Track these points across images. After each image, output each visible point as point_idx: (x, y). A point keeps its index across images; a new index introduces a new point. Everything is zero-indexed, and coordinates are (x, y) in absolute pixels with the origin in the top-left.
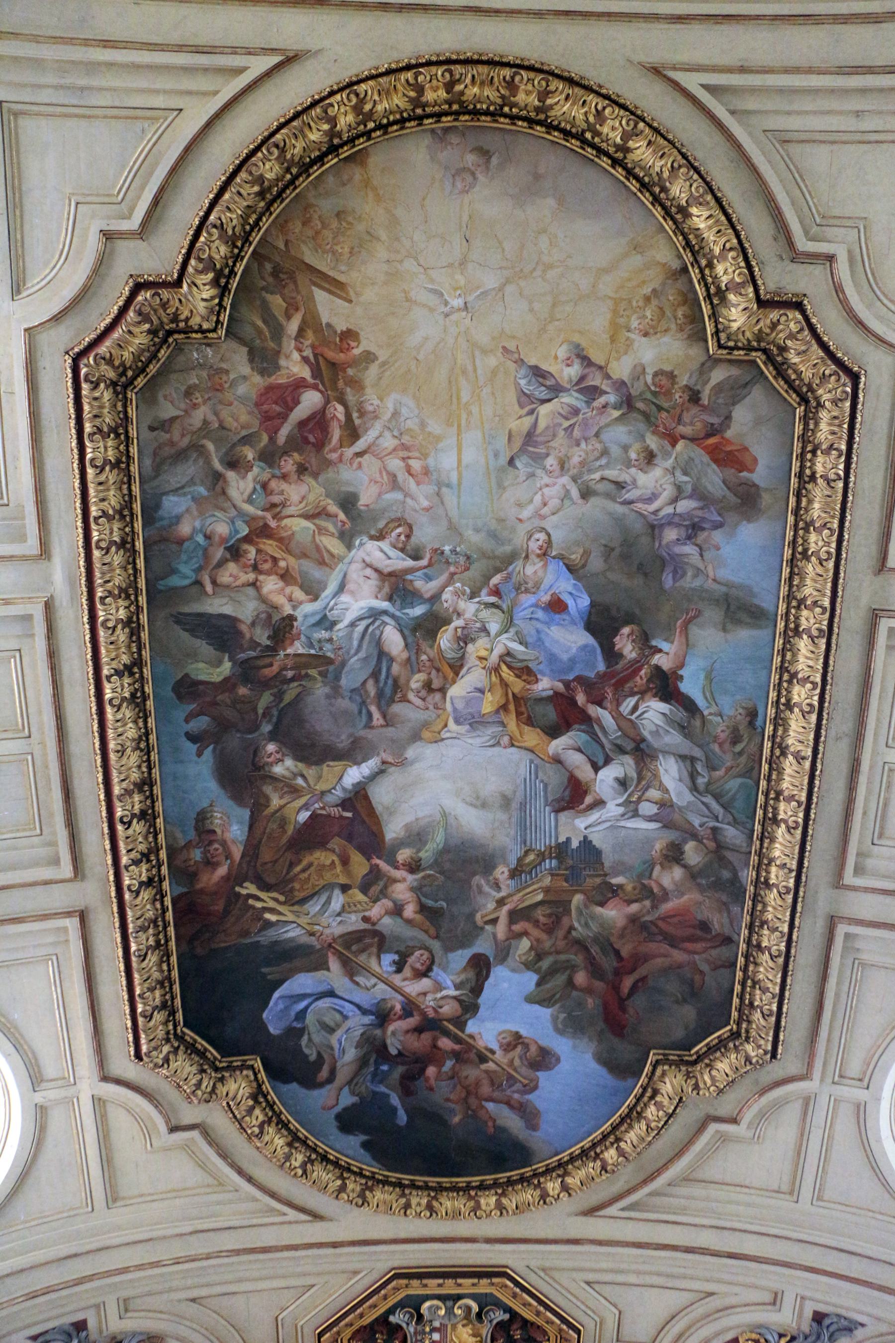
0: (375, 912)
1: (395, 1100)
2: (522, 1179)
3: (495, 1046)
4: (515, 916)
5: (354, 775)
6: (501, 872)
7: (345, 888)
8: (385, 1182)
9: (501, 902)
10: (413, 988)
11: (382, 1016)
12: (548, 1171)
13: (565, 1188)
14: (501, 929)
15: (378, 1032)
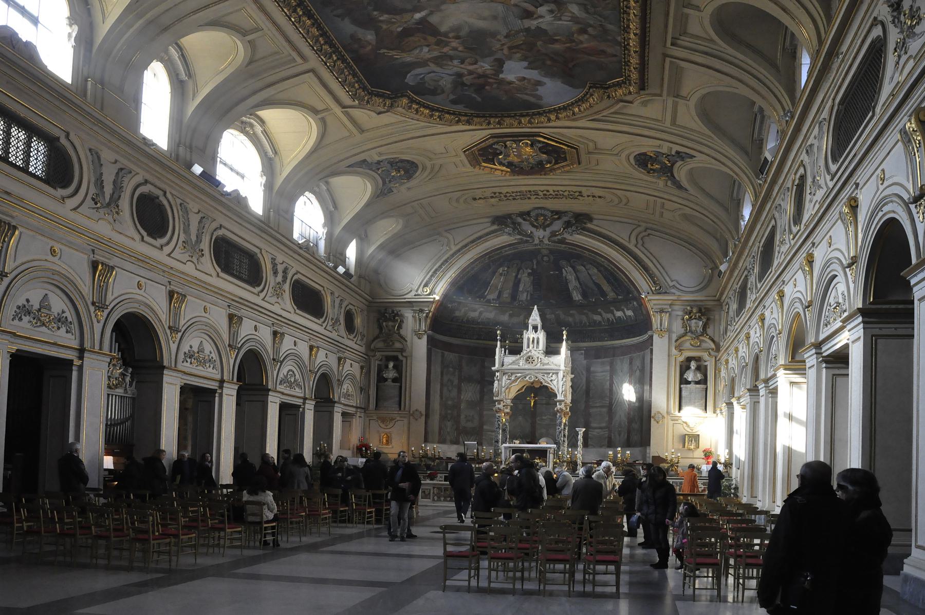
0: (445, 50)
1: (474, 95)
2: (539, 114)
3: (515, 80)
4: (510, 48)
5: (418, 16)
6: (499, 37)
7: (428, 46)
8: (478, 116)
9: (503, 45)
10: (471, 68)
11: (460, 75)
12: (550, 112)
13: (557, 118)
14: (506, 51)
15: (459, 80)
